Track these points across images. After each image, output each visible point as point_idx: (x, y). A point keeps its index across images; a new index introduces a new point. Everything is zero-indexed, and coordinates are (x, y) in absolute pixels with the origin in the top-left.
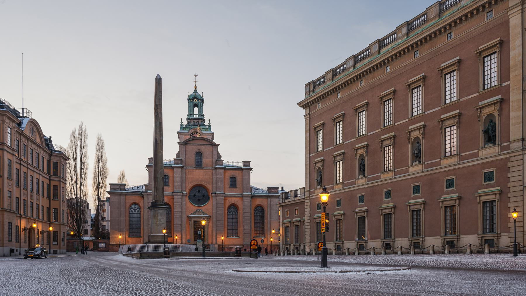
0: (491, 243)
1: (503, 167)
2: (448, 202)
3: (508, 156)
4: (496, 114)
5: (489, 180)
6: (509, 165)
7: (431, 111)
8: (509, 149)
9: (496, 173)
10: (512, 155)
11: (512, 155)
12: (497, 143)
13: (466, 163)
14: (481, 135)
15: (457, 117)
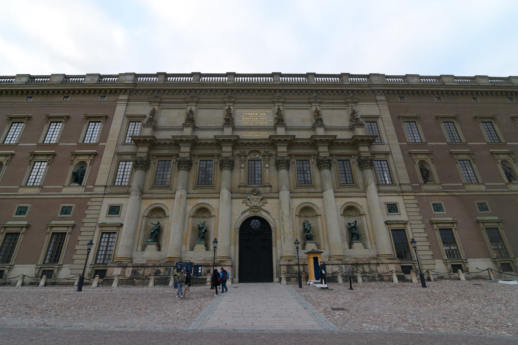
0: (49, 274)
1: (83, 204)
2: (12, 229)
3: (89, 196)
4: (88, 163)
5: (66, 214)
6: (89, 203)
7: (26, 145)
8: (92, 191)
9: (75, 208)
10: (92, 196)
11: (92, 196)
12: (82, 185)
13: (47, 195)
14: (70, 174)
15: (51, 156)
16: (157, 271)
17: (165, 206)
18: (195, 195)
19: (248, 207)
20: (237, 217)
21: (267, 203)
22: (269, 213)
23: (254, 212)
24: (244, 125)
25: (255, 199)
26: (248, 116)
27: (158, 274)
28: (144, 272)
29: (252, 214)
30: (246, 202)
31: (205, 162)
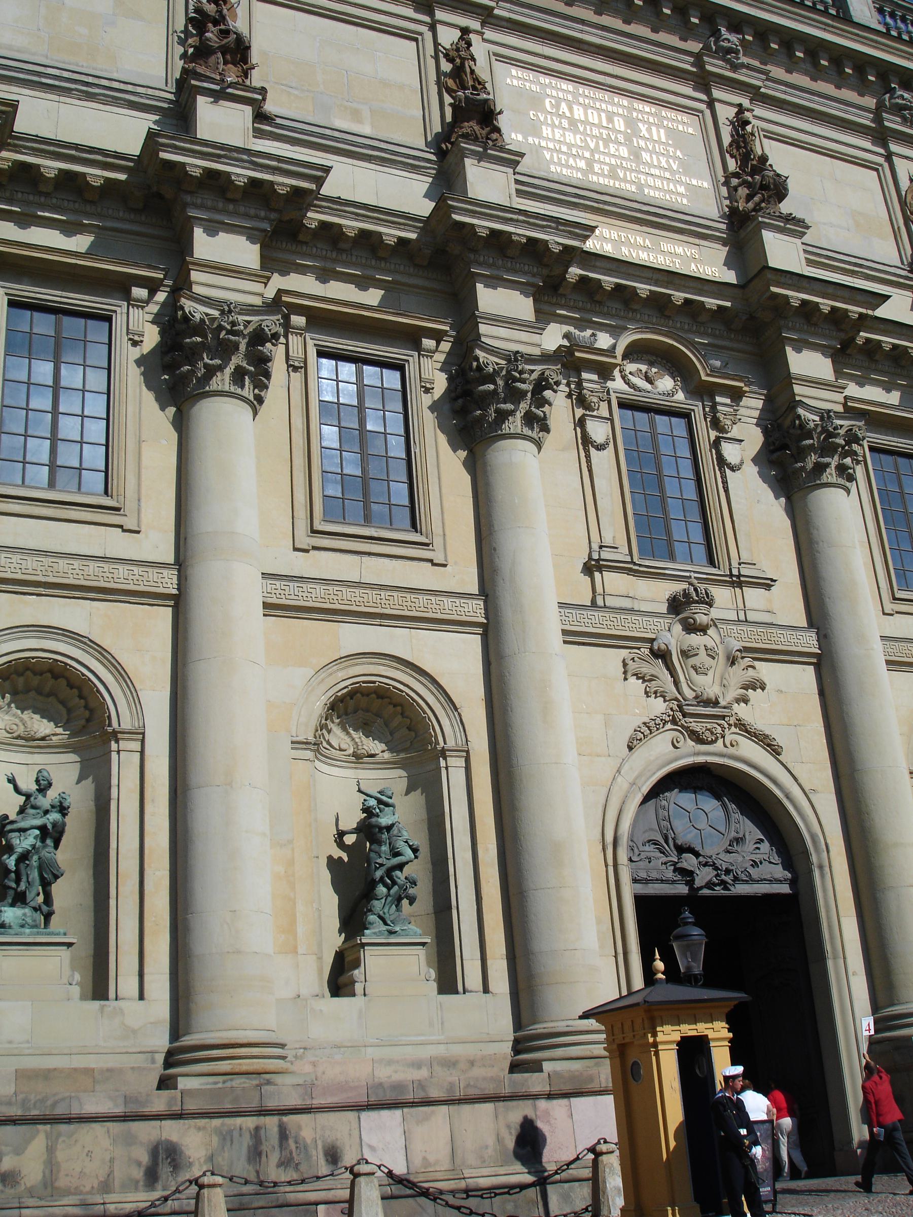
16: (154, 1152)
17: (101, 652)
18: (319, 590)
19: (659, 707)
20: (605, 768)
21: (757, 685)
22: (775, 750)
23: (697, 738)
24: (556, 170)
25: (703, 657)
26: (573, 123)
27: (164, 1170)
28: (51, 1165)
29: (690, 754)
30: (646, 669)
31: (348, 370)
